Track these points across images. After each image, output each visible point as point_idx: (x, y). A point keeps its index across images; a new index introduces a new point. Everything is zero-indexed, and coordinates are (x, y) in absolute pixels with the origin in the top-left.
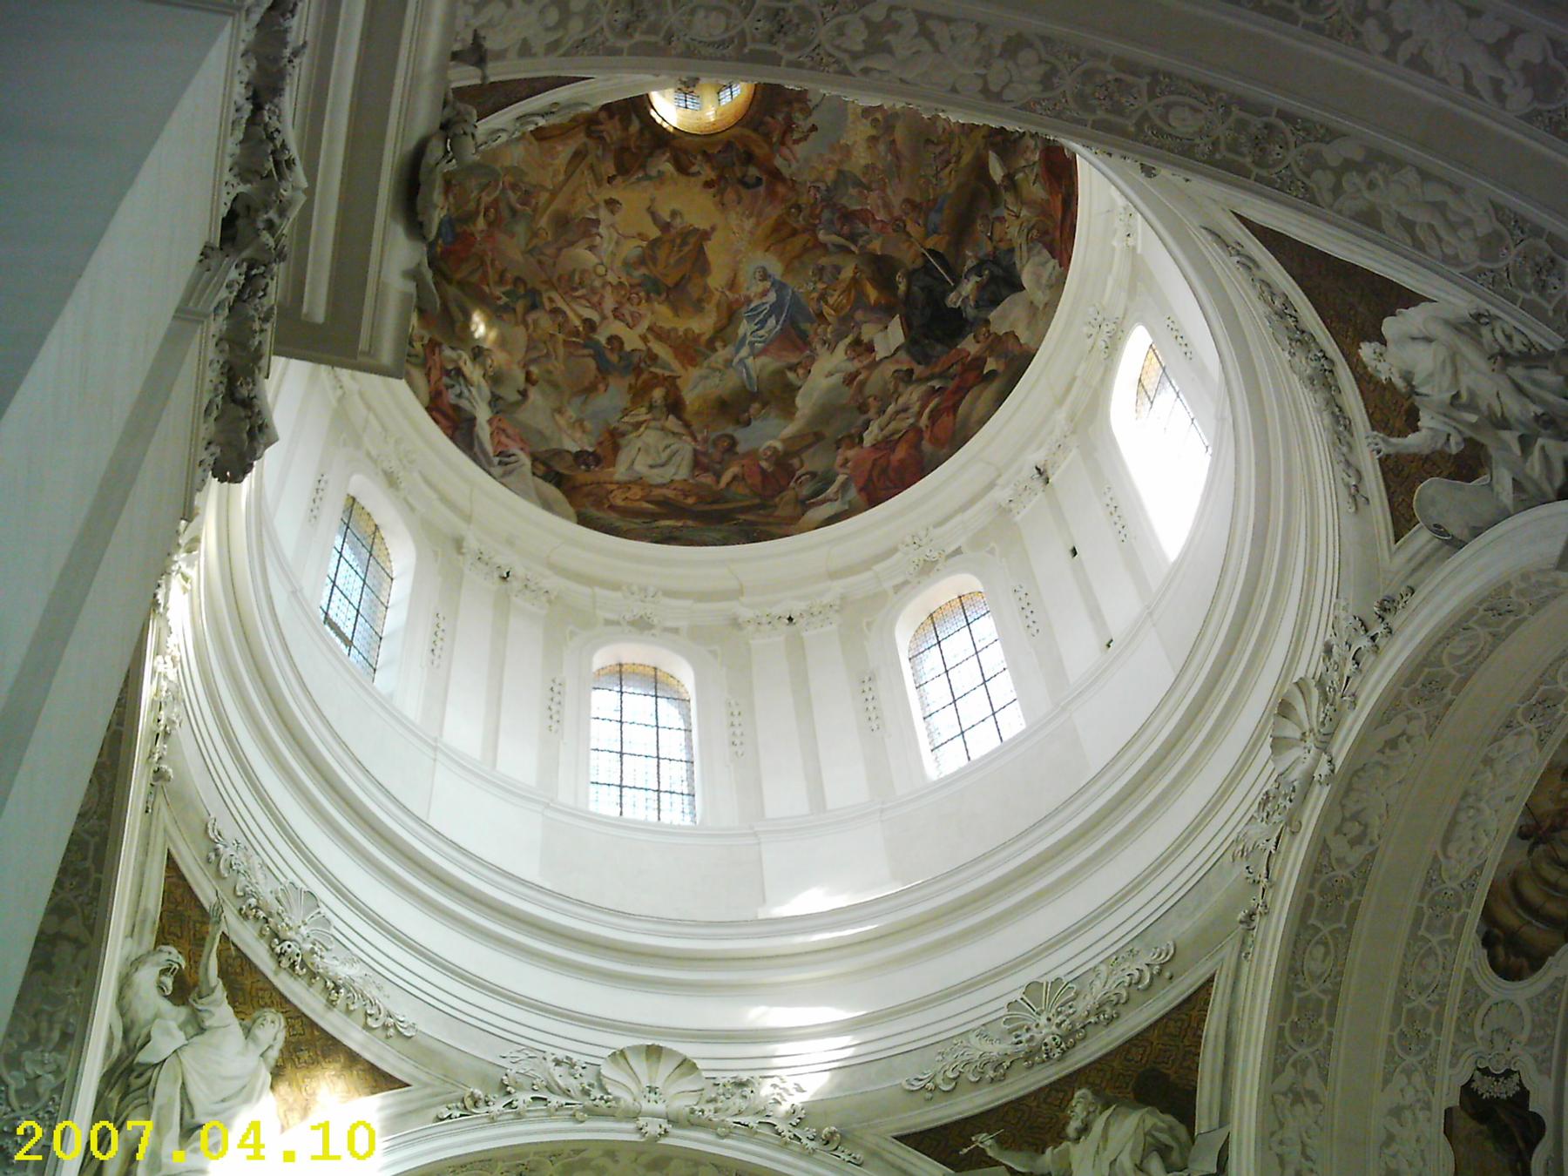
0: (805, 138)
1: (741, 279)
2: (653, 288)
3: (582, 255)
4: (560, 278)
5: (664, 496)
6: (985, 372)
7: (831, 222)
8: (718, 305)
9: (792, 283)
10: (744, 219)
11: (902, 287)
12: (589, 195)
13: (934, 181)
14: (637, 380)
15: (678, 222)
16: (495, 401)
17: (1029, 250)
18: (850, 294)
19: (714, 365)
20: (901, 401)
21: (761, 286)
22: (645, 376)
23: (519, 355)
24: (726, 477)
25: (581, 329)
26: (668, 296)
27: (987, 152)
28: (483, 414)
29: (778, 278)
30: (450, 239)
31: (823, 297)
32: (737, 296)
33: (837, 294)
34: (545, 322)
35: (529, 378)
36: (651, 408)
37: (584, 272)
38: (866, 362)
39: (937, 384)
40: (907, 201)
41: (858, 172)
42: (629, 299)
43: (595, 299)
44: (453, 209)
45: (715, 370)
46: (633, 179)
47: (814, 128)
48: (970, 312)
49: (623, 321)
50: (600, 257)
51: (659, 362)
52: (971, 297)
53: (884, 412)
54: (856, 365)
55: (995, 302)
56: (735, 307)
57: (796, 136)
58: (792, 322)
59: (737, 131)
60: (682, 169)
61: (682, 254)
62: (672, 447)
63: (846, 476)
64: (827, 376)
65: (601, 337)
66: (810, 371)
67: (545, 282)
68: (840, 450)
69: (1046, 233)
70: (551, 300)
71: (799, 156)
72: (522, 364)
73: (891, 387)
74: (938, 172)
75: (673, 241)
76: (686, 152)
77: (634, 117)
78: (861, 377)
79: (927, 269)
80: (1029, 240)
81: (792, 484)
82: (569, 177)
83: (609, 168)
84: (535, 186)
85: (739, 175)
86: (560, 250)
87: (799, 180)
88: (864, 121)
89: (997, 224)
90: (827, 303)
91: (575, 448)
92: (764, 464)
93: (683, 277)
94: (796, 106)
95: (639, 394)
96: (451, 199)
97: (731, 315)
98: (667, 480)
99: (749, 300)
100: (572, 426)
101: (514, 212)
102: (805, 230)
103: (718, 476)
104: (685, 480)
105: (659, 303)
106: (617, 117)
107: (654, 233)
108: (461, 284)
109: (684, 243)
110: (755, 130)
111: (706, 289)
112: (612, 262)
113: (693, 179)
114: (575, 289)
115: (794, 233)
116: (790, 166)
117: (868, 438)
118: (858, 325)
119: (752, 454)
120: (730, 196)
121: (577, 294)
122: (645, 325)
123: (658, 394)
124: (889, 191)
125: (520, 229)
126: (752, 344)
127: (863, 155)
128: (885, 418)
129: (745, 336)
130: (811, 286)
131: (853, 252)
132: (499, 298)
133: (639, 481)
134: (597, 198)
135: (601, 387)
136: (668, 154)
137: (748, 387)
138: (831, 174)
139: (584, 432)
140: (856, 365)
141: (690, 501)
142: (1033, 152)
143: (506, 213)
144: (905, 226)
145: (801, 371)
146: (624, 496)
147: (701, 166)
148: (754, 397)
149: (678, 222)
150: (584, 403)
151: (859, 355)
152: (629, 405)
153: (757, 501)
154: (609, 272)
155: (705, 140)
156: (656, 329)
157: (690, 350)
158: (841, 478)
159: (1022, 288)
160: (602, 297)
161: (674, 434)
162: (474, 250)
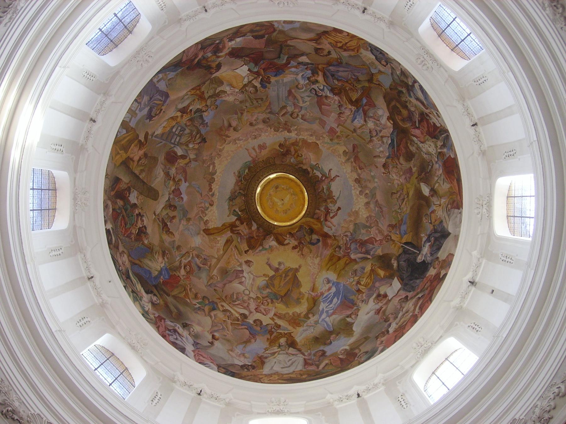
0: (336, 214)
1: (317, 285)
2: (275, 297)
3: (236, 286)
4: (226, 297)
5: (290, 377)
6: (441, 277)
7: (356, 249)
8: (308, 299)
9: (342, 282)
10: (314, 259)
11: (395, 265)
12: (236, 259)
13: (400, 211)
14: (271, 336)
15: (282, 267)
16: (195, 344)
17: (449, 216)
18: (371, 277)
19: (310, 324)
20: (404, 310)
21: (327, 286)
22: (275, 334)
23: (208, 328)
24: (321, 367)
25: (239, 318)
26: (282, 300)
27: (419, 184)
28: (190, 348)
29: (335, 280)
30: (167, 277)
31: (358, 283)
32: (316, 293)
33: (365, 279)
34: (220, 315)
35: (213, 337)
36: (280, 346)
37: (238, 294)
38: (384, 302)
39: (420, 295)
40: (390, 226)
41: (364, 221)
42: (262, 303)
43: (246, 305)
44: (167, 264)
45: (311, 326)
46: (257, 251)
47: (339, 209)
48: (429, 259)
49: (261, 313)
50: (246, 287)
51: (281, 327)
52: (428, 253)
53: (397, 317)
54: (380, 304)
55: (439, 249)
56: (316, 298)
57: (331, 215)
58: (345, 297)
59: (304, 220)
60: (281, 243)
61: (286, 280)
62: (292, 360)
63: (383, 347)
64: (366, 314)
65: (251, 321)
66: (358, 315)
67: (219, 299)
68: (378, 339)
69: (454, 202)
70: (222, 306)
71: (334, 224)
72: (210, 332)
73: (399, 307)
74: (400, 206)
75: (281, 276)
76: (281, 235)
77: (253, 223)
78: (383, 309)
79: (405, 252)
80: (448, 211)
81: (356, 359)
82: (225, 253)
83: (245, 247)
84: (209, 257)
85: (308, 240)
86: (225, 285)
87: (336, 235)
88: (361, 196)
89: (432, 215)
90: (360, 284)
91: (241, 364)
92: (341, 356)
93: (289, 290)
94: (328, 201)
95: (272, 342)
96: (166, 259)
97: (314, 302)
98: (291, 371)
99: (322, 294)
100: (239, 356)
101: (199, 268)
102: (344, 256)
103: (318, 366)
104: (301, 370)
105: (278, 303)
106: (245, 223)
107: (272, 273)
108: (175, 297)
109: (286, 276)
110: (313, 218)
111: (300, 293)
112: (252, 288)
113: (286, 247)
114: (236, 301)
115: (339, 259)
116: (332, 230)
117: (391, 330)
118: (378, 289)
119: (335, 355)
120: (306, 250)
121: (236, 303)
122: (271, 314)
123: (282, 341)
124: (380, 225)
125: (204, 275)
126: (327, 312)
127: (364, 212)
128: (398, 320)
129: (323, 309)
130: (352, 279)
131: (369, 259)
132: (196, 305)
133: (277, 373)
134: (240, 261)
135: (253, 340)
136: (273, 237)
137: (328, 329)
138: (351, 227)
139: (245, 357)
140: (380, 304)
141: (304, 377)
142: (439, 170)
143: (195, 268)
144: (391, 237)
145: (353, 316)
146: (268, 379)
147: (289, 240)
148: (331, 333)
149: (282, 267)
150: (244, 347)
151: (380, 301)
152: (268, 346)
153: (340, 369)
154: (251, 293)
155: (290, 227)
156: (278, 314)
157: (296, 321)
158: (380, 348)
159: (449, 234)
160: (249, 304)
161: (293, 355)
162: (180, 283)
